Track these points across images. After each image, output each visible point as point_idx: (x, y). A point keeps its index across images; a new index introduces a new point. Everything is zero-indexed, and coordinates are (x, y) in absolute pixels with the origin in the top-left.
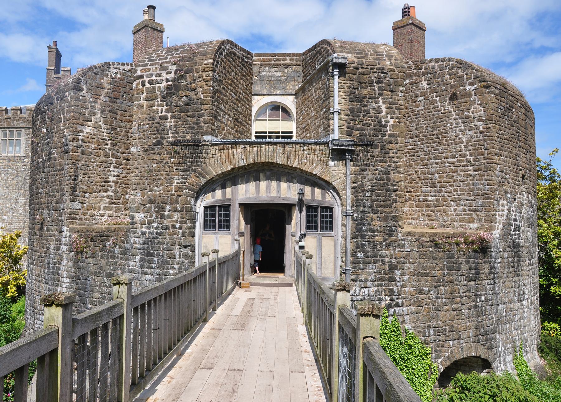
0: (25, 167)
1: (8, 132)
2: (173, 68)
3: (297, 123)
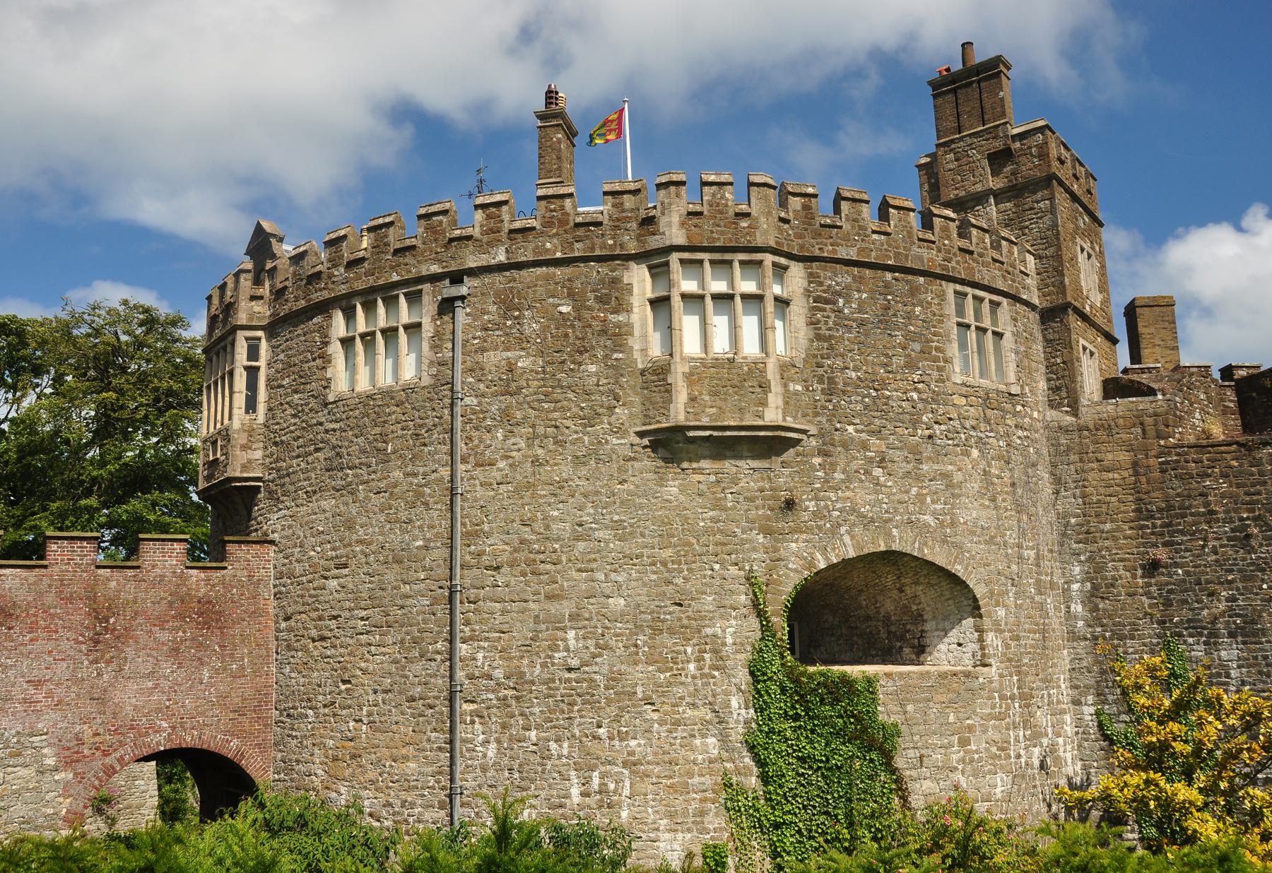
0: (1020, 433)
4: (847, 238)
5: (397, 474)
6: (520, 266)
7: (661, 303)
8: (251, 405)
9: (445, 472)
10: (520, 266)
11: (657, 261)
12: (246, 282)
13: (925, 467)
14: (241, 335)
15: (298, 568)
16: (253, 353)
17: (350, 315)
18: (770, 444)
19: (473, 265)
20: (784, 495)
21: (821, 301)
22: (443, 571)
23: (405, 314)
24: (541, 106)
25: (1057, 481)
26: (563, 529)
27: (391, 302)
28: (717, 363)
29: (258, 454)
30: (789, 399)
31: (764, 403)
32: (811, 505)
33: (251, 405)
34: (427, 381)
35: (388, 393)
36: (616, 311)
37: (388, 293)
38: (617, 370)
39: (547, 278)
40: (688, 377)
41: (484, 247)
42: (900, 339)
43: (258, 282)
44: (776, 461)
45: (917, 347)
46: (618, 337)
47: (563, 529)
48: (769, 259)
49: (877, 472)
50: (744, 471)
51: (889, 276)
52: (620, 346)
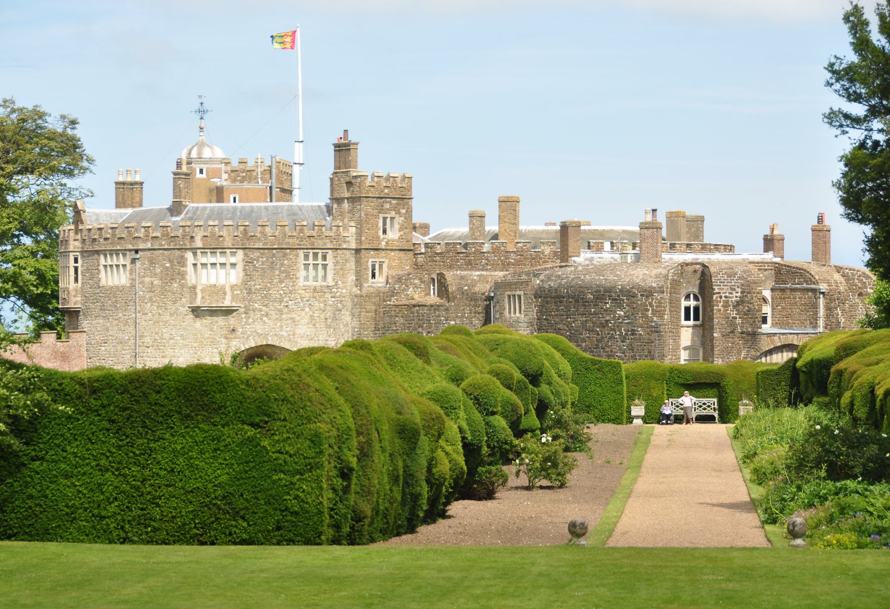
1: (311, 256)
2: (739, 290)
3: (773, 309)
4: (259, 239)
5: (121, 315)
6: (154, 250)
7: (195, 265)
8: (76, 280)
9: (134, 316)
10: (154, 250)
11: (194, 251)
12: (72, 234)
13: (284, 316)
14: (71, 254)
15: (93, 342)
16: (76, 261)
17: (106, 257)
18: (228, 312)
19: (141, 247)
20: (232, 327)
21: (248, 262)
22: (133, 347)
23: (122, 261)
24: (174, 169)
25: (353, 315)
26: (167, 336)
27: (117, 255)
28: (211, 286)
29: (79, 299)
30: (234, 297)
31: (224, 299)
32: (241, 330)
33: (76, 280)
34: (128, 285)
35: (117, 287)
36: (183, 267)
37: (117, 252)
38: (182, 286)
39: (163, 254)
40: (203, 291)
41: (145, 241)
42: (277, 272)
43: (76, 233)
44: (230, 317)
45: (284, 275)
46: (183, 275)
47: (167, 336)
48: (228, 251)
49: (265, 319)
50: (220, 320)
51: (274, 251)
52: (183, 278)
